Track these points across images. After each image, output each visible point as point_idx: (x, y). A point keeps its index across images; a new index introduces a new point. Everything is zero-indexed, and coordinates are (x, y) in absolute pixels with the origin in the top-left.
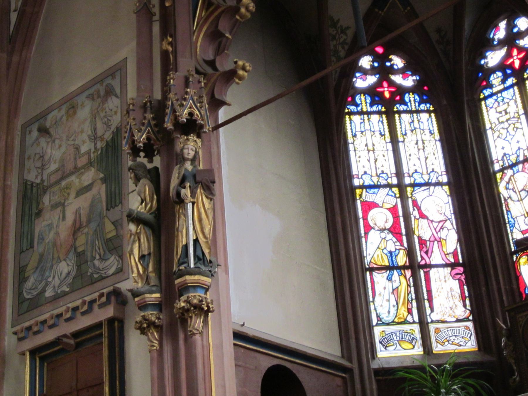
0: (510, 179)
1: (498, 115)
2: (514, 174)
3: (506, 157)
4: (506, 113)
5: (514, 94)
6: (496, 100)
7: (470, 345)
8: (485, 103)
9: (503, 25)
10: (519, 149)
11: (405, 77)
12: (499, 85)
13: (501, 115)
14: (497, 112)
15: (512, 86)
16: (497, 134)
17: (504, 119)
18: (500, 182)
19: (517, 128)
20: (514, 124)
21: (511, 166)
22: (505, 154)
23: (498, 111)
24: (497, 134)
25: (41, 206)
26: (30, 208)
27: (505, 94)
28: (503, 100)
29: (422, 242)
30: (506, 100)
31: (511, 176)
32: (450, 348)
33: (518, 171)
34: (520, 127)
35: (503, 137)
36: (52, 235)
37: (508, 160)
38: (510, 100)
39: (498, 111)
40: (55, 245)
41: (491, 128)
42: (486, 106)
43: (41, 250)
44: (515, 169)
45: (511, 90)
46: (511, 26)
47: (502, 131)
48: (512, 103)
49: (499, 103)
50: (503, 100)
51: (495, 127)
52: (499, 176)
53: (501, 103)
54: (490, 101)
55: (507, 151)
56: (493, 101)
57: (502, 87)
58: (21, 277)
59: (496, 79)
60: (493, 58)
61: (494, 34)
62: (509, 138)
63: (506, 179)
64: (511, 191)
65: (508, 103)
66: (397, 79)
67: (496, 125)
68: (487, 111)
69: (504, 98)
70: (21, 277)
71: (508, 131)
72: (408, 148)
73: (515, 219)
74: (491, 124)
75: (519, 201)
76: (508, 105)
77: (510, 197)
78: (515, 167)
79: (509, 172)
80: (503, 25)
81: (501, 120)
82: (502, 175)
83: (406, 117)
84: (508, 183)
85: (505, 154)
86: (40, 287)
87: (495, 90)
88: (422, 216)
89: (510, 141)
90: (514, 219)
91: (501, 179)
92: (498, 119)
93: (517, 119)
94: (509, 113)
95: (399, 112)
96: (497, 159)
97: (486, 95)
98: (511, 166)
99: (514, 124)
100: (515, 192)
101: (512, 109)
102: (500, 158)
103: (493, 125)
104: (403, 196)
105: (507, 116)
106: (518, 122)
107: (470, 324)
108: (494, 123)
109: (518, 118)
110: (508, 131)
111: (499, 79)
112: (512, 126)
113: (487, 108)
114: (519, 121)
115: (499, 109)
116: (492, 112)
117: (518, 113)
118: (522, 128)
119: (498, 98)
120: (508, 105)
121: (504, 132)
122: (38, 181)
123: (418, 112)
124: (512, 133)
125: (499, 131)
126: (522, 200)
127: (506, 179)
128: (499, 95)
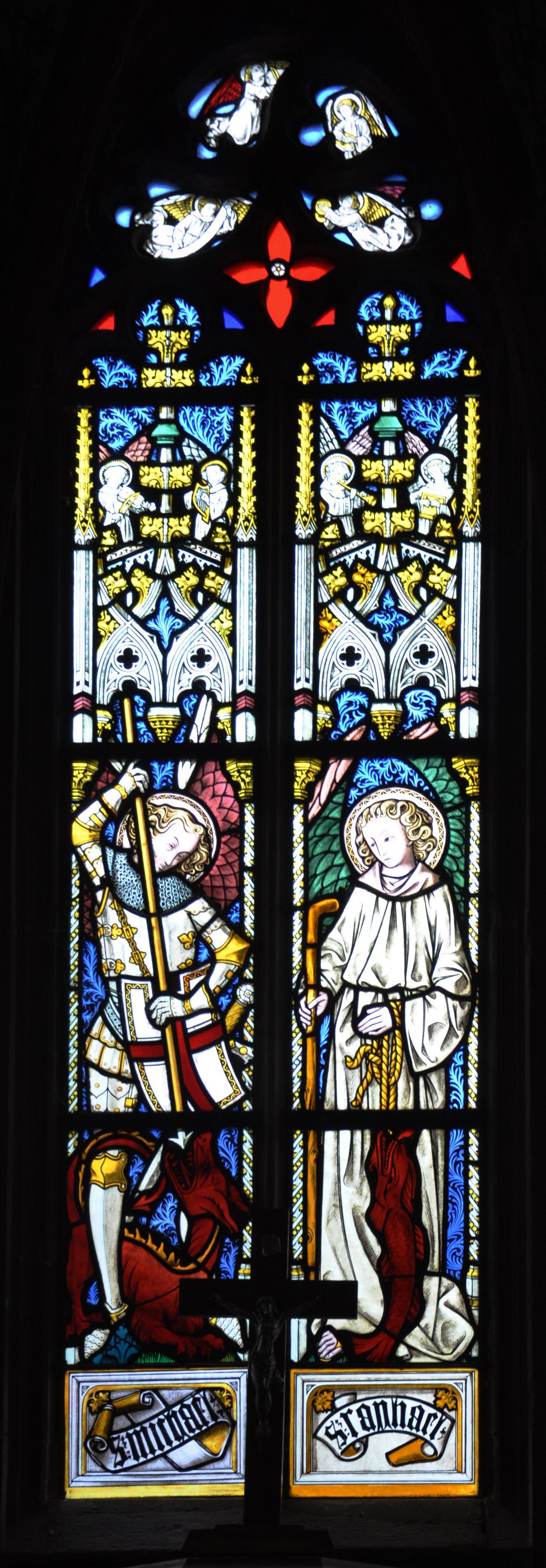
0: (127, 804)
1: (138, 502)
2: (151, 791)
3: (134, 705)
4: (178, 510)
5: (236, 434)
6: (146, 430)
8: (94, 422)
10: (198, 688)
12: (176, 365)
13: (152, 507)
14: (136, 485)
15: (230, 396)
16: (115, 584)
18: (84, 804)
19: (212, 597)
20: (202, 574)
21: (147, 753)
22: (130, 688)
23: (144, 481)
24: (115, 584)
27: (192, 418)
28: (176, 444)
30: (190, 451)
31: (135, 793)
33: (171, 787)
34: (227, 597)
35: (140, 610)
37: (135, 720)
38: (211, 456)
39: (144, 481)
41: (93, 546)
42: (93, 435)
44: (161, 772)
45: (225, 415)
47: (140, 580)
48: (214, 473)
49: (155, 447)
50: (176, 444)
51: (113, 549)
53: (166, 455)
54: (120, 420)
55: (145, 674)
56: (132, 430)
57: (183, 378)
59: (169, 329)
61: (210, 111)
62: (164, 626)
63: (112, 797)
64: (122, 859)
65: (197, 467)
67: (120, 544)
68: (96, 464)
69: (183, 435)
71: (165, 593)
73: (113, 985)
74: (100, 527)
75: (144, 913)
76: (197, 478)
77: (109, 882)
78: (162, 762)
79: (132, 778)
81: (149, 527)
82: (96, 777)
84: (113, 817)
85: (130, 688)
87: (153, 378)
89: (166, 637)
90: (106, 981)
91: (92, 792)
92: (135, 518)
93: (218, 557)
94: (193, 513)
96: (92, 697)
97: (109, 381)
98: (147, 753)
99: (202, 574)
100: (138, 869)
102: (104, 697)
103: (109, 540)
105: (181, 526)
106: (220, 572)
108: (114, 527)
109: (225, 554)
110: (165, 593)
111: (182, 339)
112: (190, 579)
113: (94, 449)
114: (228, 570)
115: (151, 477)
116: (115, 473)
117: (230, 528)
118: (232, 607)
119: (158, 421)
120: (197, 478)
121: (150, 590)
124: (187, 610)
125: (127, 576)
126: (161, 913)
127: (112, 797)
128: (165, 413)
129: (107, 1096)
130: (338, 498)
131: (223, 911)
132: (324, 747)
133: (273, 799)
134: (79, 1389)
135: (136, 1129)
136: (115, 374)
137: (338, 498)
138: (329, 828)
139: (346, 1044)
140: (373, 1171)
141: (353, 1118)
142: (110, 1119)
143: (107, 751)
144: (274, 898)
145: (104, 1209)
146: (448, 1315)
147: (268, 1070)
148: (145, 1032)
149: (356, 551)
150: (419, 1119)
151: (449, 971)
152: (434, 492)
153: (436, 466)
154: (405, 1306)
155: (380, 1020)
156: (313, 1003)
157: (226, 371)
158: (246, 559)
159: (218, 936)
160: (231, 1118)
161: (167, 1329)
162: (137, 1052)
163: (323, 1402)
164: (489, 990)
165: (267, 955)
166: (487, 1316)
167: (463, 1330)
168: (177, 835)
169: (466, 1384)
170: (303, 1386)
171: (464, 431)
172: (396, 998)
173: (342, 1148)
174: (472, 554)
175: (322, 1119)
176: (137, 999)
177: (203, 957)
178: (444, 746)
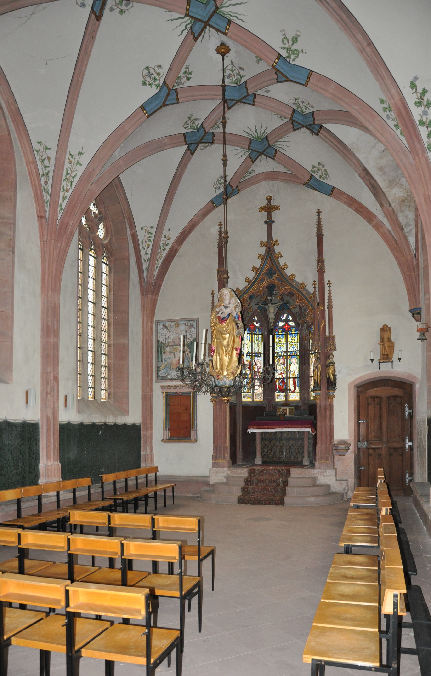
7: (262, 400)
9: (285, 315)
11: (257, 323)
15: (284, 334)
17: (280, 342)
25: (165, 350)
26: (161, 349)
29: (255, 372)
32: (257, 400)
36: (170, 360)
40: (171, 364)
43: (166, 363)
46: (287, 317)
52: (276, 357)
54: (277, 336)
58: (158, 369)
59: (280, 331)
60: (281, 324)
66: (255, 323)
70: (158, 369)
72: (255, 345)
79: (279, 358)
80: (285, 315)
83: (256, 336)
86: (166, 374)
88: (256, 365)
95: (254, 334)
101: (283, 341)
104: (252, 359)
107: (262, 394)
122: (164, 342)
123: (259, 334)
129: (277, 377)
130: (291, 340)
131: (284, 365)
132: (290, 355)
133: (287, 359)
134: (276, 394)
135: (279, 379)
136: (277, 333)
137: (291, 340)
138: (290, 360)
139: (291, 373)
140: (293, 381)
141: (292, 378)
142: (278, 378)
143: (277, 356)
144: (287, 365)
145: (277, 384)
146: (298, 389)
147: (287, 375)
148: (280, 373)
149: (291, 343)
150: (296, 378)
151: (298, 369)
152: (296, 340)
153: (296, 338)
154: (295, 389)
155: (293, 372)
156: (289, 371)
157: (284, 333)
158: (285, 344)
159: (284, 367)
160: (285, 378)
161: (281, 391)
162: (279, 374)
163: (290, 395)
164: (300, 370)
165: (287, 368)
166: (300, 389)
167: (298, 391)
168: (281, 361)
169: (299, 393)
170: (289, 394)
171: (298, 336)
172: (294, 371)
173: (291, 380)
174: (298, 343)
175: (290, 378)
176: (279, 371)
177: (283, 368)
178: (297, 355)
